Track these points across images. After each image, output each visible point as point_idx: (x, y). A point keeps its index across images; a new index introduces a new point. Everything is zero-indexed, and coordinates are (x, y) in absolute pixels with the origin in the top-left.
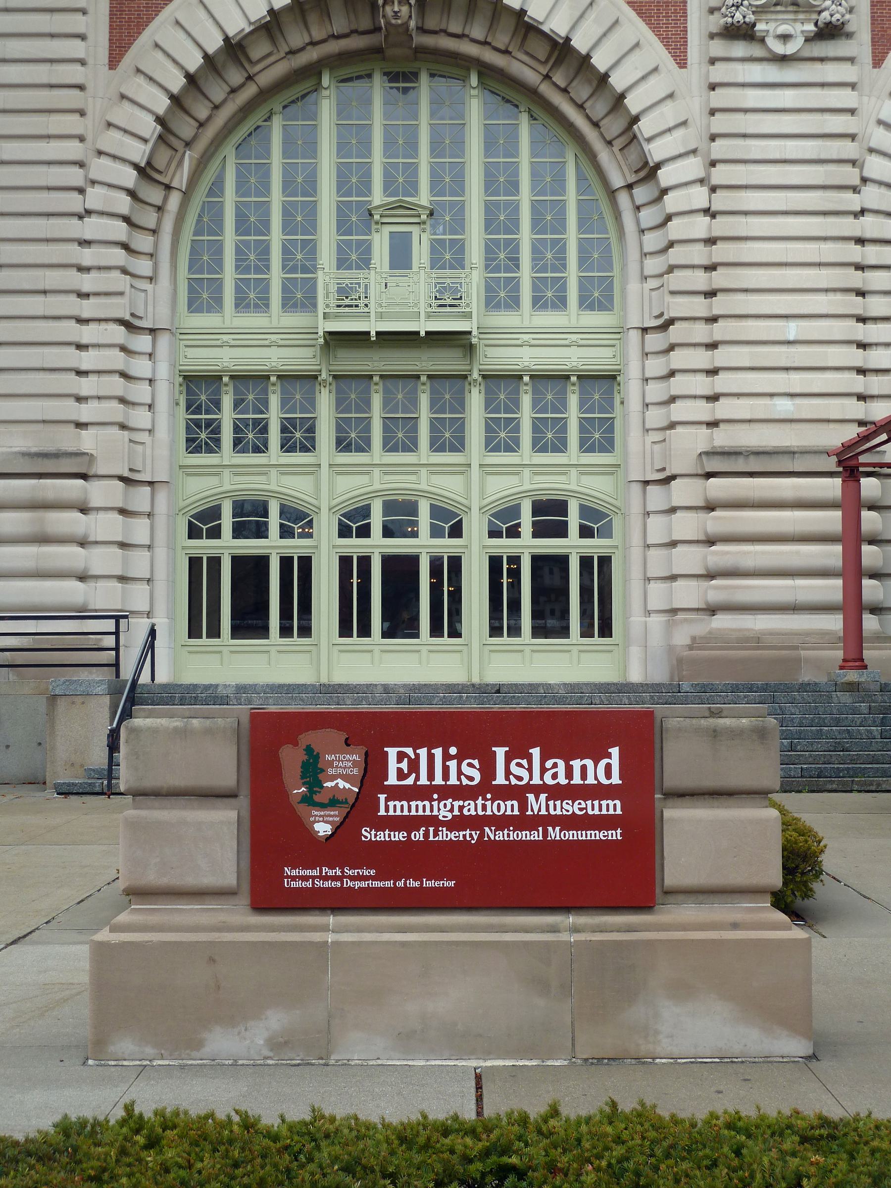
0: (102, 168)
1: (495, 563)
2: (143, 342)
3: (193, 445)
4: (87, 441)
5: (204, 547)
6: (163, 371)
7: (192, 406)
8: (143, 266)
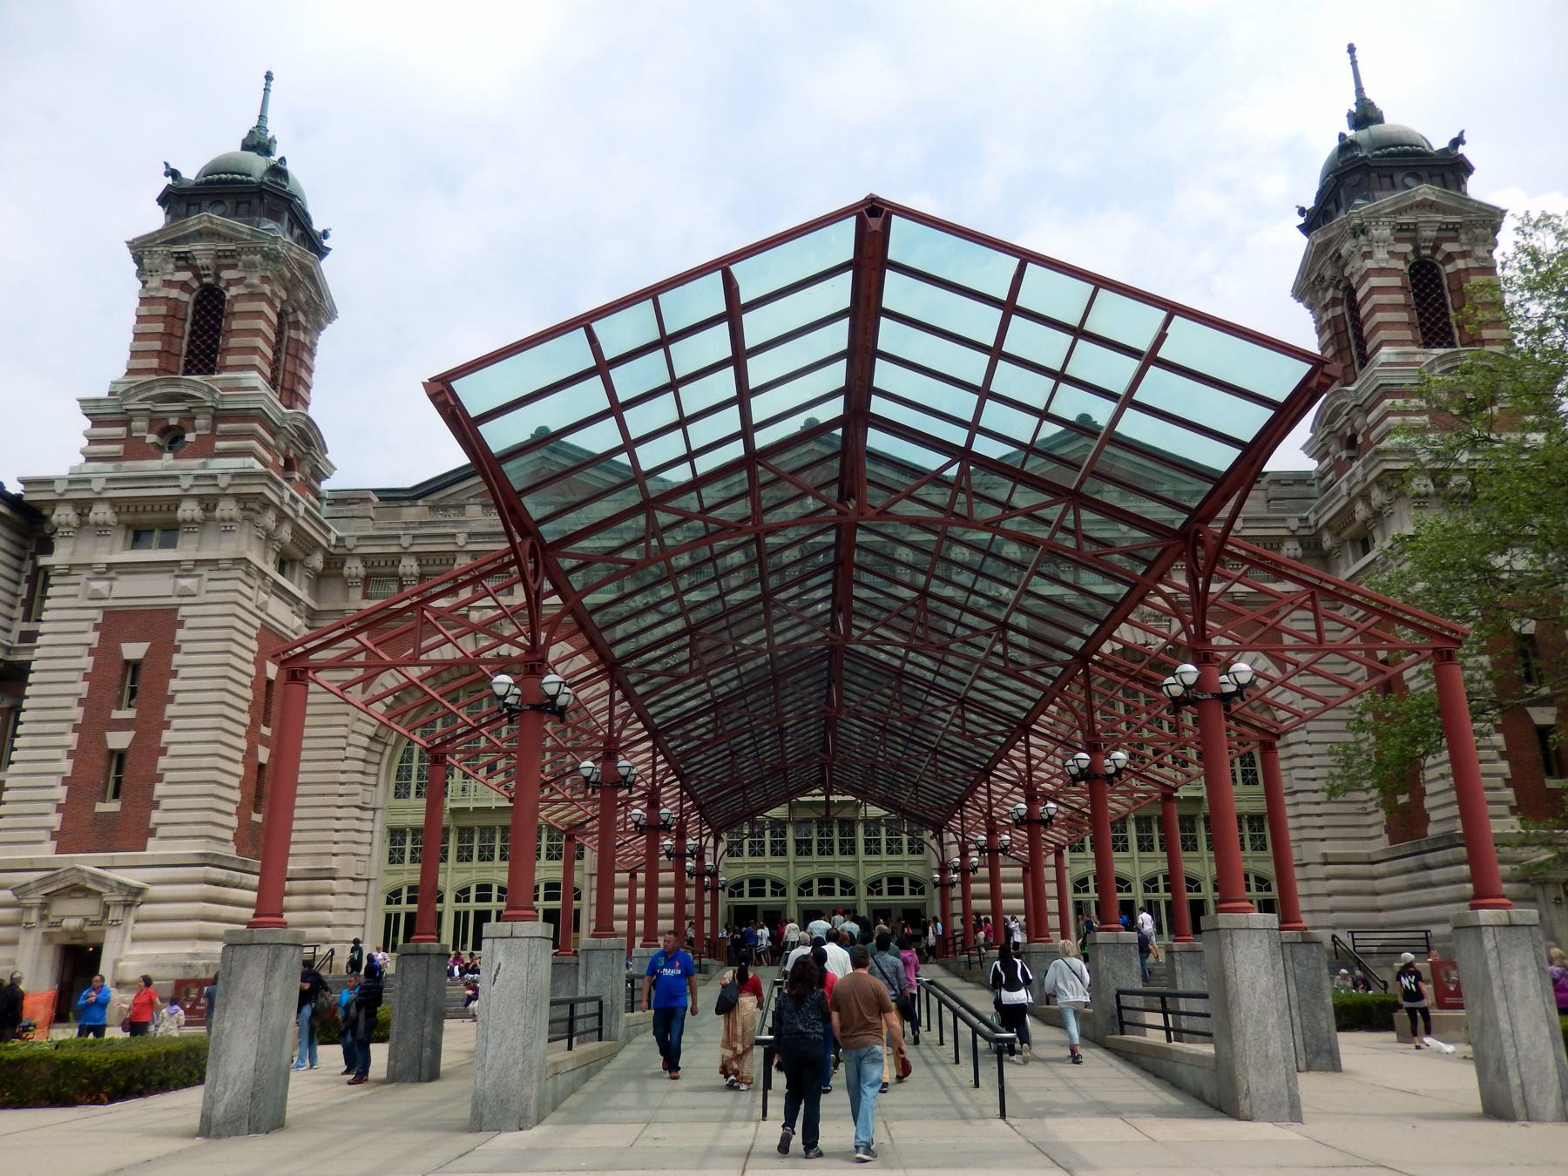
0: (354, 739)
2: (369, 815)
3: (392, 861)
4: (334, 863)
5: (393, 908)
6: (378, 826)
7: (393, 842)
8: (372, 780)
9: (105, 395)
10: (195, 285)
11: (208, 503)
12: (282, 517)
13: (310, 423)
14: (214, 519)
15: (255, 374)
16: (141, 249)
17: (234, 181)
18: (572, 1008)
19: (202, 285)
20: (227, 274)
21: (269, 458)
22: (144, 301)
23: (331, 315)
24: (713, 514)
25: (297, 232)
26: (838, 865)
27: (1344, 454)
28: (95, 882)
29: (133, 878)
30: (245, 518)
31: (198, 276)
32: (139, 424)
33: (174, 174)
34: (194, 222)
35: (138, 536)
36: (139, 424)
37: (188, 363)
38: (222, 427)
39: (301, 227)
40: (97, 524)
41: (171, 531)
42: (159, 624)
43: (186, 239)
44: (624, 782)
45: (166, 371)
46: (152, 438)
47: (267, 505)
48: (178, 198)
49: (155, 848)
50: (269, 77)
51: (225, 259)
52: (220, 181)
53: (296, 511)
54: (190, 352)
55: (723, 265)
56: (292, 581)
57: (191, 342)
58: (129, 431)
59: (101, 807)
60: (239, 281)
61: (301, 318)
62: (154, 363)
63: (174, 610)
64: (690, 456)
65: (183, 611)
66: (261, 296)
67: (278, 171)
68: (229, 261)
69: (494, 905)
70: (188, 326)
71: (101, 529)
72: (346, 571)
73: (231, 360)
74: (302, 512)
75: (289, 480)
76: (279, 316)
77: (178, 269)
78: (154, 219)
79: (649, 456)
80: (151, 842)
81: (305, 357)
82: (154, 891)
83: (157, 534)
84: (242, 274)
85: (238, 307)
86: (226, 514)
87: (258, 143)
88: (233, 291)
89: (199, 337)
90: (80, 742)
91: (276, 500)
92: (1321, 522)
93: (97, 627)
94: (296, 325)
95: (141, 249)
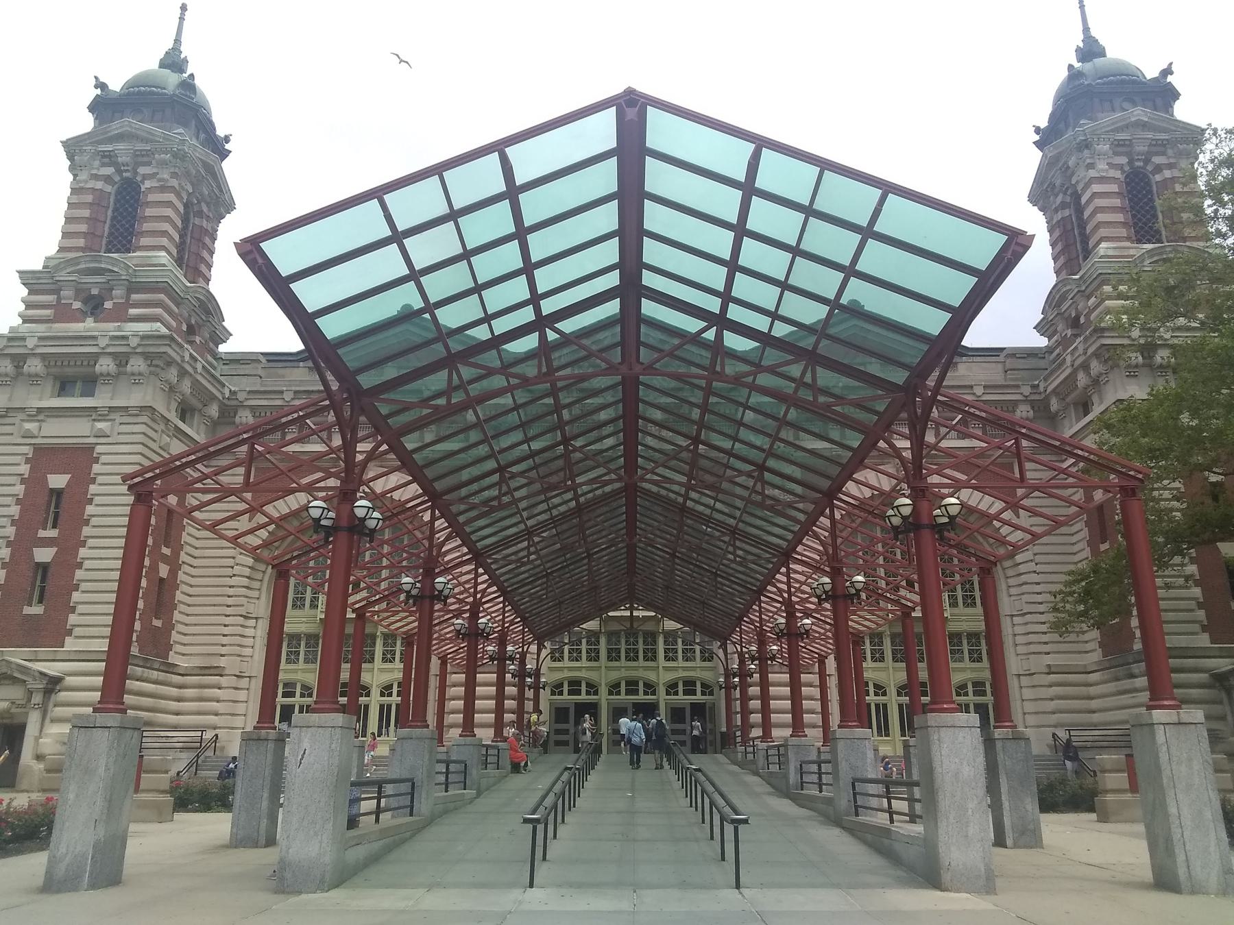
1: (382, 706)
2: (252, 622)
4: (222, 662)
8: (255, 594)
9: (40, 267)
10: (117, 178)
11: (122, 360)
12: (183, 373)
13: (211, 298)
14: (125, 374)
15: (163, 253)
16: (73, 147)
17: (153, 93)
18: (380, 788)
19: (122, 179)
20: (142, 170)
21: (174, 324)
22: (75, 191)
23: (230, 206)
24: (513, 370)
25: (202, 136)
26: (641, 670)
27: (1069, 332)
28: (21, 673)
29: (53, 669)
30: (151, 373)
31: (119, 172)
32: (67, 293)
33: (101, 85)
34: (116, 127)
35: (64, 386)
36: (67, 293)
37: (109, 243)
38: (134, 297)
39: (206, 132)
40: (30, 375)
41: (90, 383)
42: (80, 458)
43: (111, 140)
44: (442, 597)
45: (91, 250)
46: (77, 305)
47: (170, 363)
48: (105, 105)
49: (70, 644)
50: (184, 8)
51: (142, 158)
52: (139, 93)
53: (195, 369)
54: (111, 234)
55: (499, 147)
56: (191, 426)
57: (112, 226)
58: (59, 299)
59: (28, 610)
60: (152, 176)
61: (205, 209)
62: (81, 242)
63: (90, 448)
64: (488, 319)
65: (99, 449)
66: (172, 189)
67: (189, 86)
68: (145, 159)
69: (297, 700)
70: (110, 213)
71: (34, 379)
72: (237, 420)
73: (145, 241)
74: (200, 369)
75: (191, 343)
76: (186, 206)
77: (103, 165)
78: (85, 123)
79: (450, 317)
80: (68, 640)
81: (207, 240)
82: (70, 681)
83: (79, 385)
84: (155, 170)
85: (152, 197)
86: (136, 369)
87: (174, 61)
88: (148, 184)
89: (119, 222)
90: (12, 555)
91: (178, 359)
92: (1050, 389)
93: (27, 461)
94: (200, 214)
95: (73, 147)
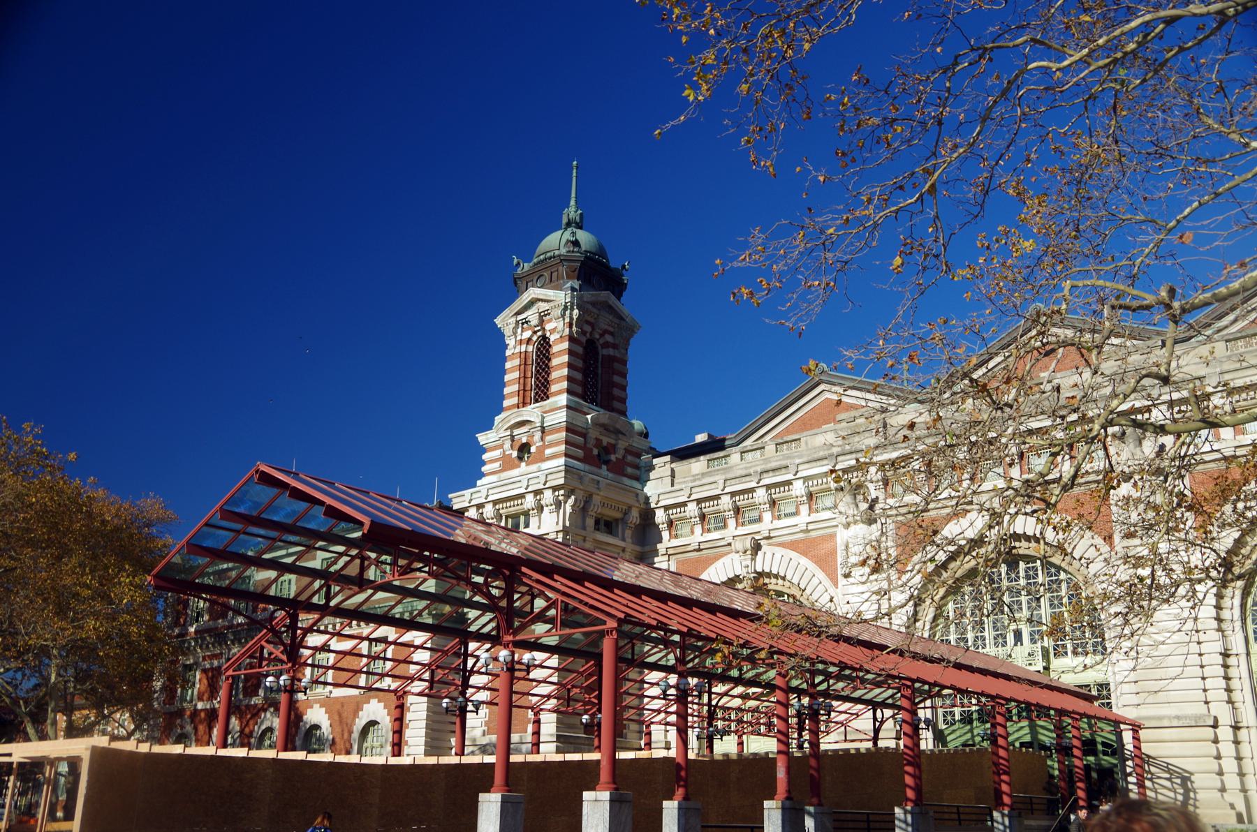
61: (608, 338)
